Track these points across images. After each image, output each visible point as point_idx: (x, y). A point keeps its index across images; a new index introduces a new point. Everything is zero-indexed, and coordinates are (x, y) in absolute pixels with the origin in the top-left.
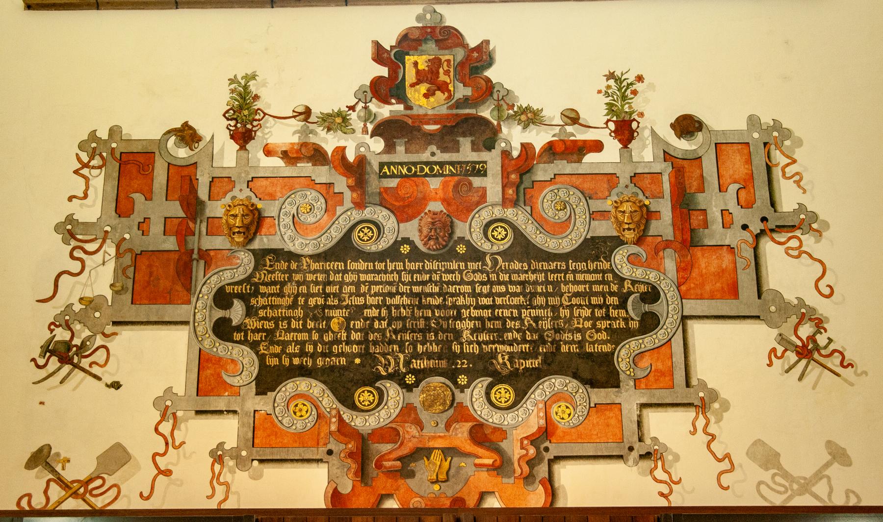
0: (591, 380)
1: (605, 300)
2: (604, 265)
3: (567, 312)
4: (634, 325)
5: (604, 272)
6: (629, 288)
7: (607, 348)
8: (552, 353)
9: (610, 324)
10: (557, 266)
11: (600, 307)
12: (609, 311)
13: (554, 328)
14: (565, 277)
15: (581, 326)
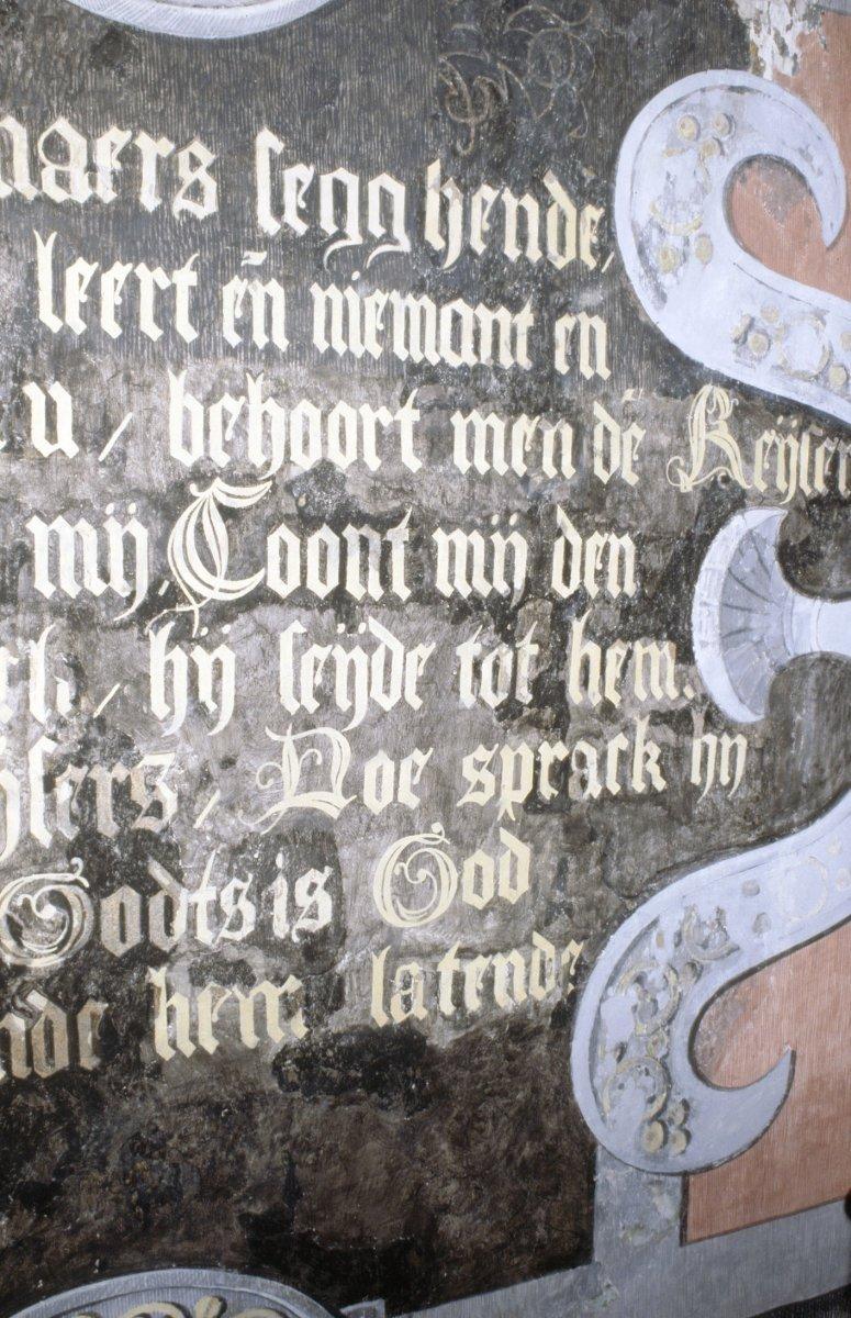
0: (394, 1255)
1: (540, 562)
2: (551, 225)
3: (220, 665)
4: (718, 763)
5: (551, 291)
6: (715, 455)
7: (520, 980)
8: (70, 1078)
9: (561, 771)
10: (127, 179)
11: (502, 617)
12: (560, 656)
13: (87, 843)
14: (205, 307)
15: (331, 803)
